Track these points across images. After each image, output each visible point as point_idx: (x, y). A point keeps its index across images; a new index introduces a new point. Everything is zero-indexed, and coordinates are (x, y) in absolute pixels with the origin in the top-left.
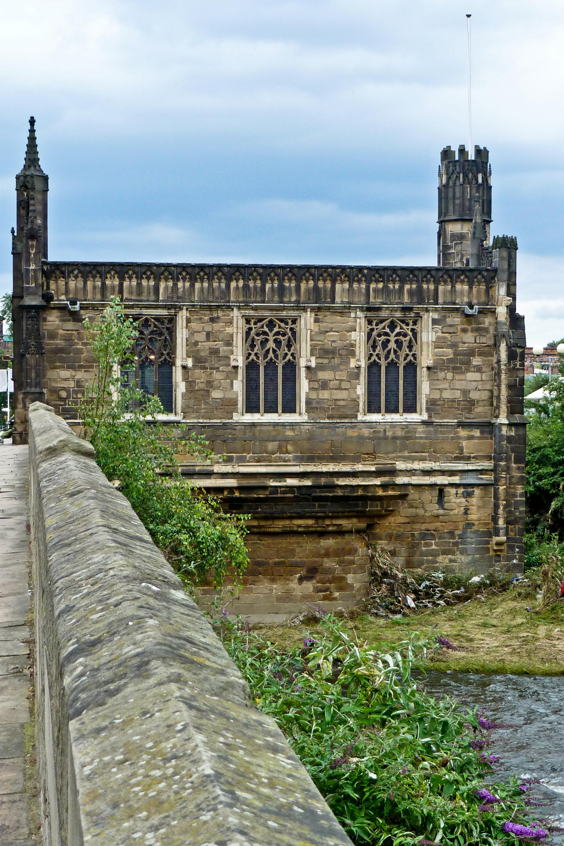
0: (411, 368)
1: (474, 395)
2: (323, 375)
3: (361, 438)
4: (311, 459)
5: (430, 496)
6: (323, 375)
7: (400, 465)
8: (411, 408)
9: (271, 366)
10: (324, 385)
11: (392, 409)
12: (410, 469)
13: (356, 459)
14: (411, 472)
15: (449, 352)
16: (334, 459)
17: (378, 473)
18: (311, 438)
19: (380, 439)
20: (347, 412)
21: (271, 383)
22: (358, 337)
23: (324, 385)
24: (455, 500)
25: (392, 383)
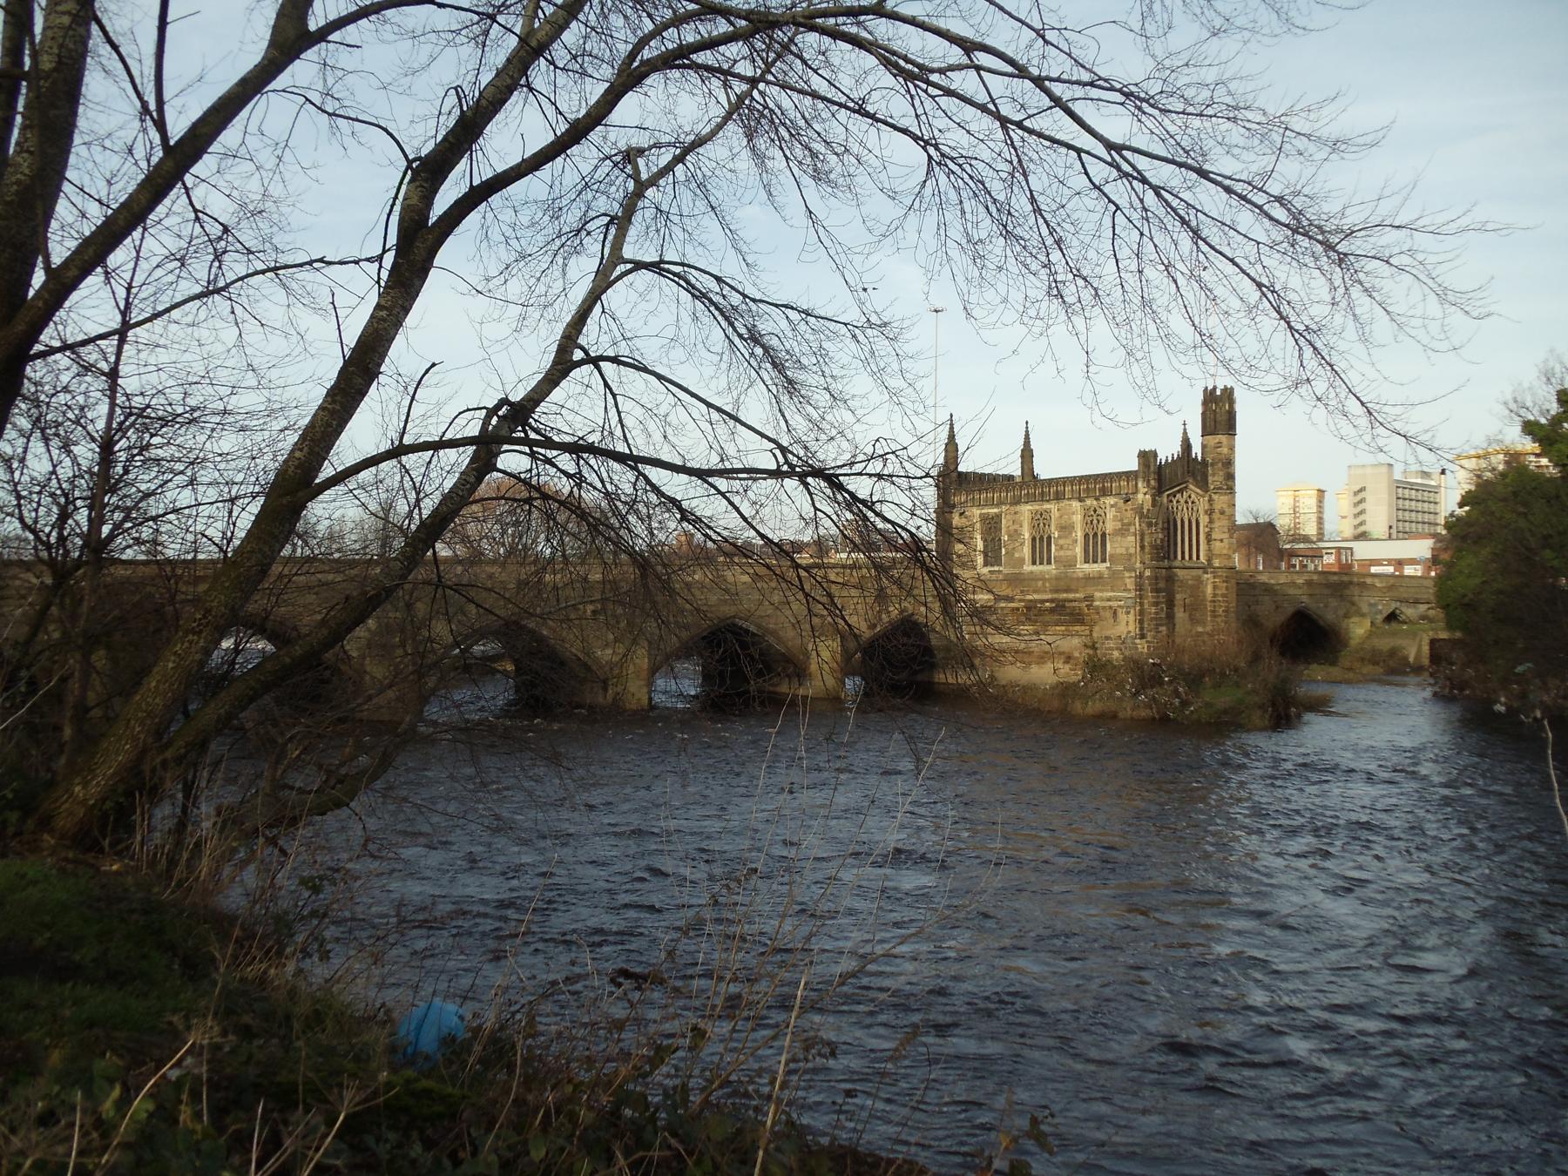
0: (1104, 535)
1: (1132, 551)
2: (1061, 542)
3: (1078, 579)
4: (1057, 591)
5: (1108, 614)
6: (1061, 542)
7: (1097, 594)
8: (1104, 561)
9: (1041, 538)
10: (1062, 548)
11: (1095, 562)
12: (1101, 596)
13: (1076, 591)
14: (1102, 600)
15: (1119, 525)
16: (1067, 591)
17: (1086, 599)
18: (1057, 578)
19: (1088, 579)
20: (1071, 563)
21: (1041, 547)
22: (1078, 519)
23: (1062, 548)
24: (1122, 616)
25: (1095, 545)
